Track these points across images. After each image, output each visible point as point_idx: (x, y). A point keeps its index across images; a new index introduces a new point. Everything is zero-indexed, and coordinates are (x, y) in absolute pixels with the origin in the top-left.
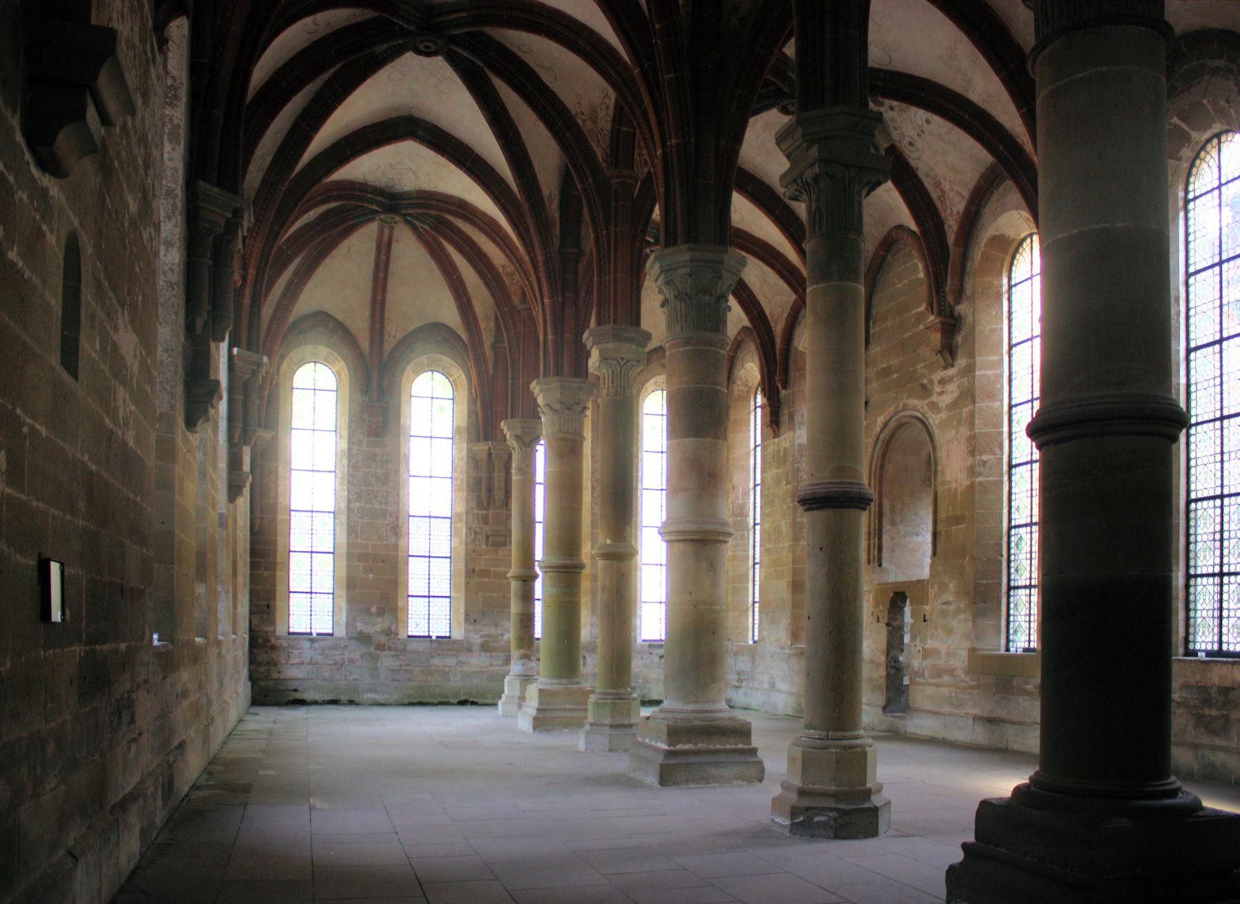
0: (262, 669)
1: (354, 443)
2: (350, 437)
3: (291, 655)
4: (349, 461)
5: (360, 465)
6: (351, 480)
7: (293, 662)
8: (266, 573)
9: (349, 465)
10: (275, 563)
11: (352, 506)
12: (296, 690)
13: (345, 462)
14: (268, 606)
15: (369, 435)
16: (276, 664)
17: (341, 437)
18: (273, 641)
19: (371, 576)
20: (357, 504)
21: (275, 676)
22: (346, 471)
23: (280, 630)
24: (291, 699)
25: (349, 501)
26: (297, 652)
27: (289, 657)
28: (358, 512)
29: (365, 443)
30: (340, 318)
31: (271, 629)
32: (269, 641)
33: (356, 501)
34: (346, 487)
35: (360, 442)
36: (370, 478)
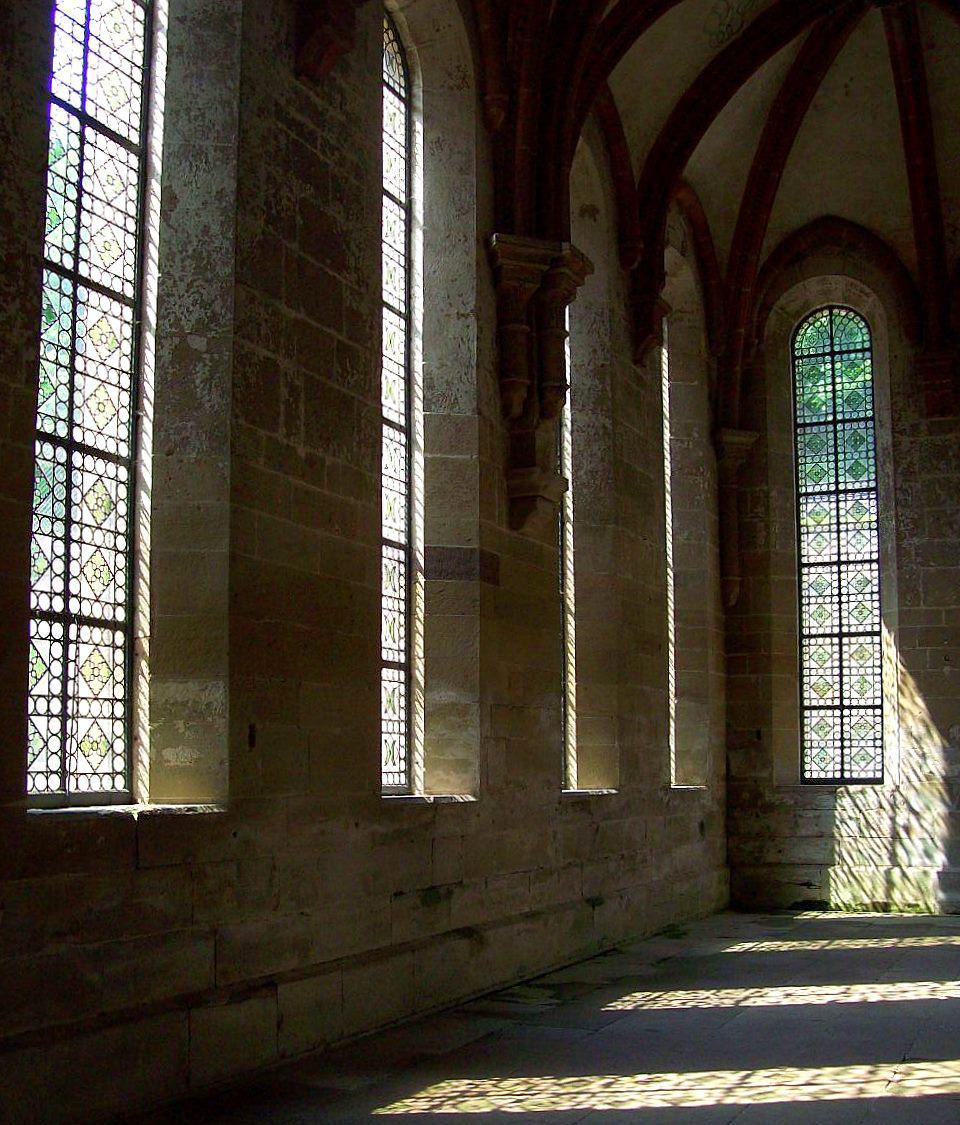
0: (748, 847)
1: (901, 433)
2: (895, 421)
3: (800, 821)
4: (896, 464)
5: (916, 467)
6: (901, 497)
7: (803, 832)
8: (753, 677)
9: (895, 470)
10: (769, 657)
11: (905, 543)
12: (808, 885)
13: (889, 468)
14: (759, 735)
15: (930, 414)
16: (772, 838)
17: (881, 426)
18: (768, 797)
19: (947, 669)
20: (915, 540)
21: (771, 857)
22: (892, 484)
23: (780, 771)
24: (800, 900)
25: (899, 537)
26: (811, 814)
27: (796, 822)
28: (917, 555)
29: (923, 428)
30: (862, 218)
31: (765, 774)
32: (760, 795)
33: (912, 536)
34: (893, 513)
35: (915, 427)
36: (939, 491)
